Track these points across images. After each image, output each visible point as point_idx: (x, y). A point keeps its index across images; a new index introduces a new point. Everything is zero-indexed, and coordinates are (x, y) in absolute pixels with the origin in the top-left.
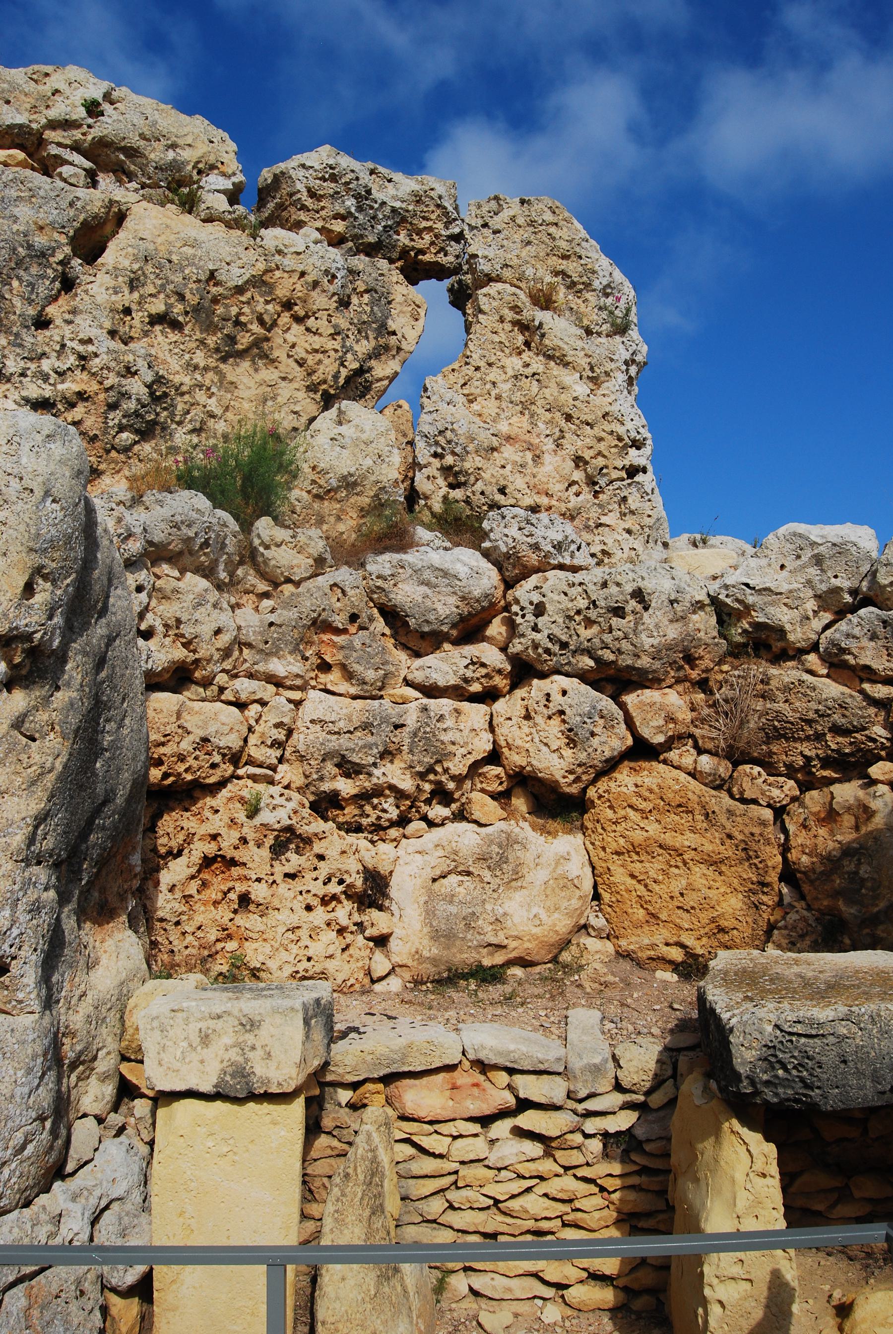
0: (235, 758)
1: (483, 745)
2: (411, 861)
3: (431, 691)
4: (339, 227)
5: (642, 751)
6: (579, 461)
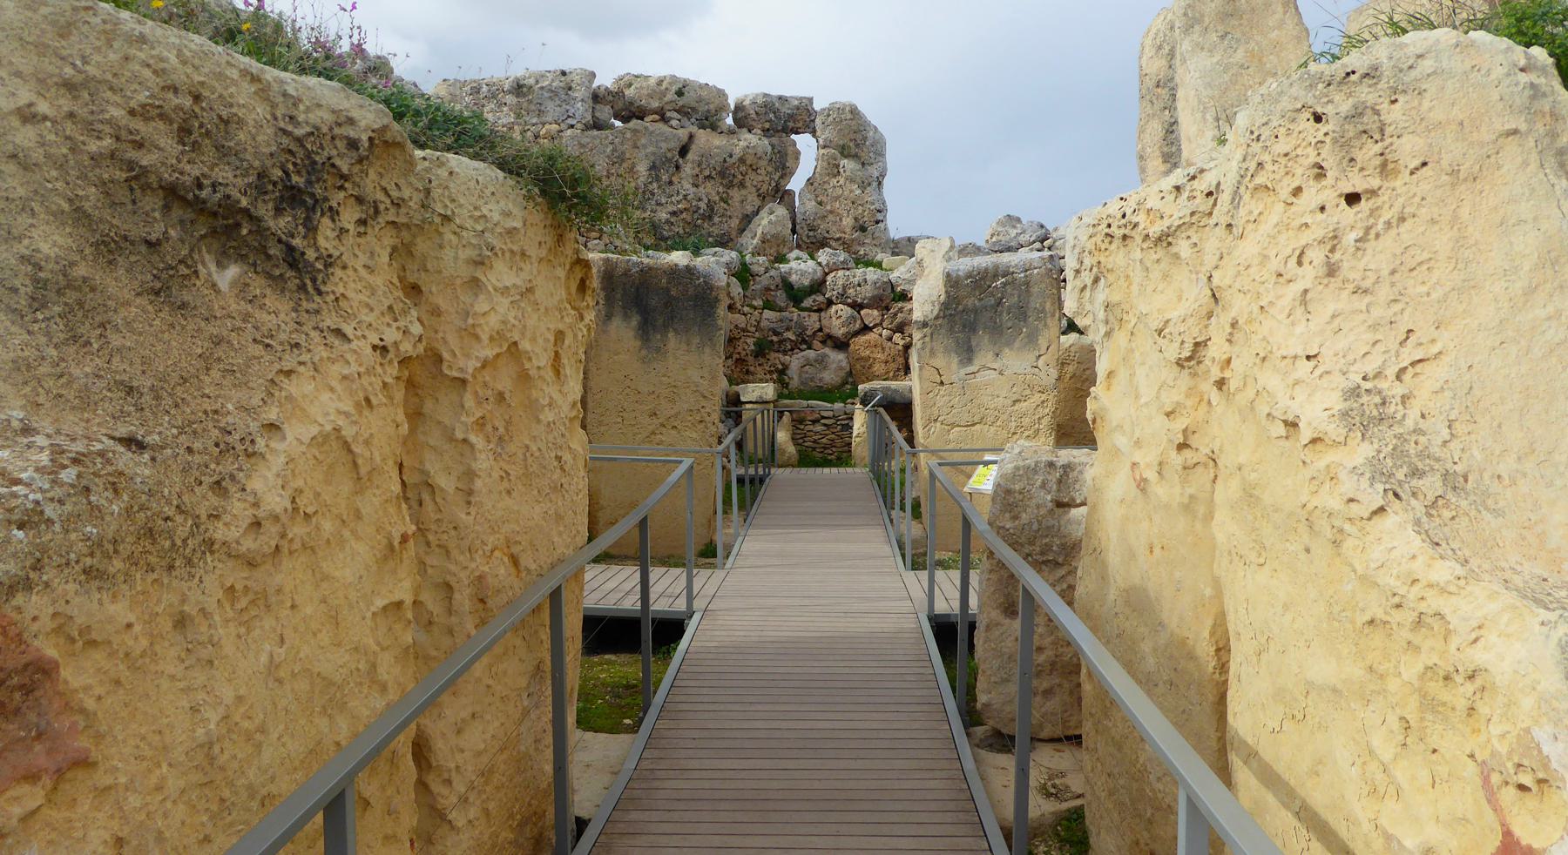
0: (744, 330)
1: (817, 326)
2: (795, 361)
4: (767, 125)
5: (866, 329)
6: (856, 219)
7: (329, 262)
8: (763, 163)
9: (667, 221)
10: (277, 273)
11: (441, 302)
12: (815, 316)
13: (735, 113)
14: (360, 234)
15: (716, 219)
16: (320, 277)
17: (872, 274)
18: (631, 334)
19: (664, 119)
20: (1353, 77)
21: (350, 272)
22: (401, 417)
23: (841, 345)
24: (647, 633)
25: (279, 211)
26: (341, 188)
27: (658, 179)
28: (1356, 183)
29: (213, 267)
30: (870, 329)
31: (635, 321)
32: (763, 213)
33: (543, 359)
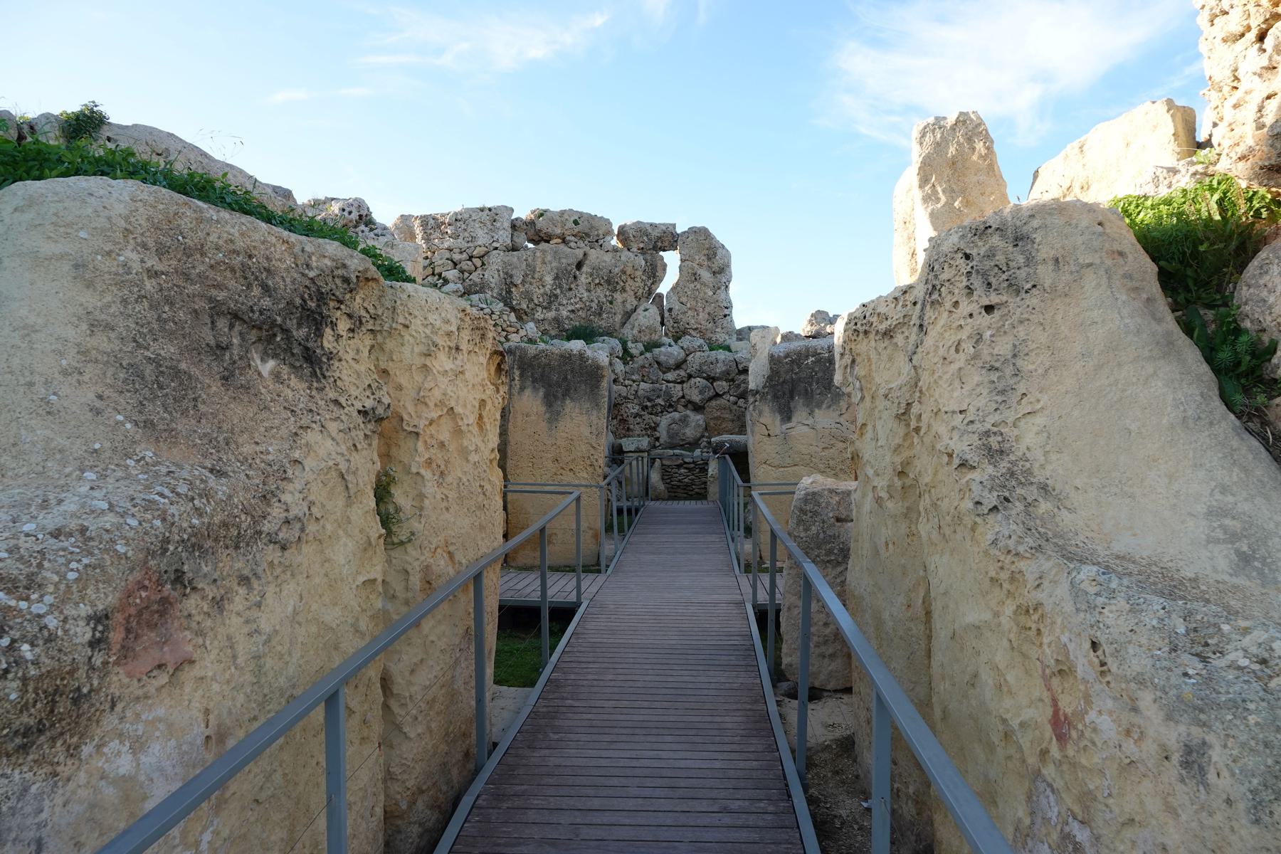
0: (626, 398)
2: (664, 421)
3: (668, 382)
5: (717, 395)
7: (330, 356)
8: (639, 273)
9: (568, 317)
10: (298, 364)
11: (403, 380)
12: (679, 387)
13: (618, 236)
14: (350, 338)
15: (605, 316)
16: (325, 367)
17: (722, 355)
18: (539, 402)
19: (564, 241)
20: (990, 231)
21: (344, 363)
22: (376, 458)
23: (698, 408)
24: (545, 614)
25: (299, 325)
26: (338, 308)
27: (561, 287)
28: (994, 299)
29: (259, 362)
30: (721, 396)
31: (541, 394)
32: (640, 310)
33: (472, 419)
